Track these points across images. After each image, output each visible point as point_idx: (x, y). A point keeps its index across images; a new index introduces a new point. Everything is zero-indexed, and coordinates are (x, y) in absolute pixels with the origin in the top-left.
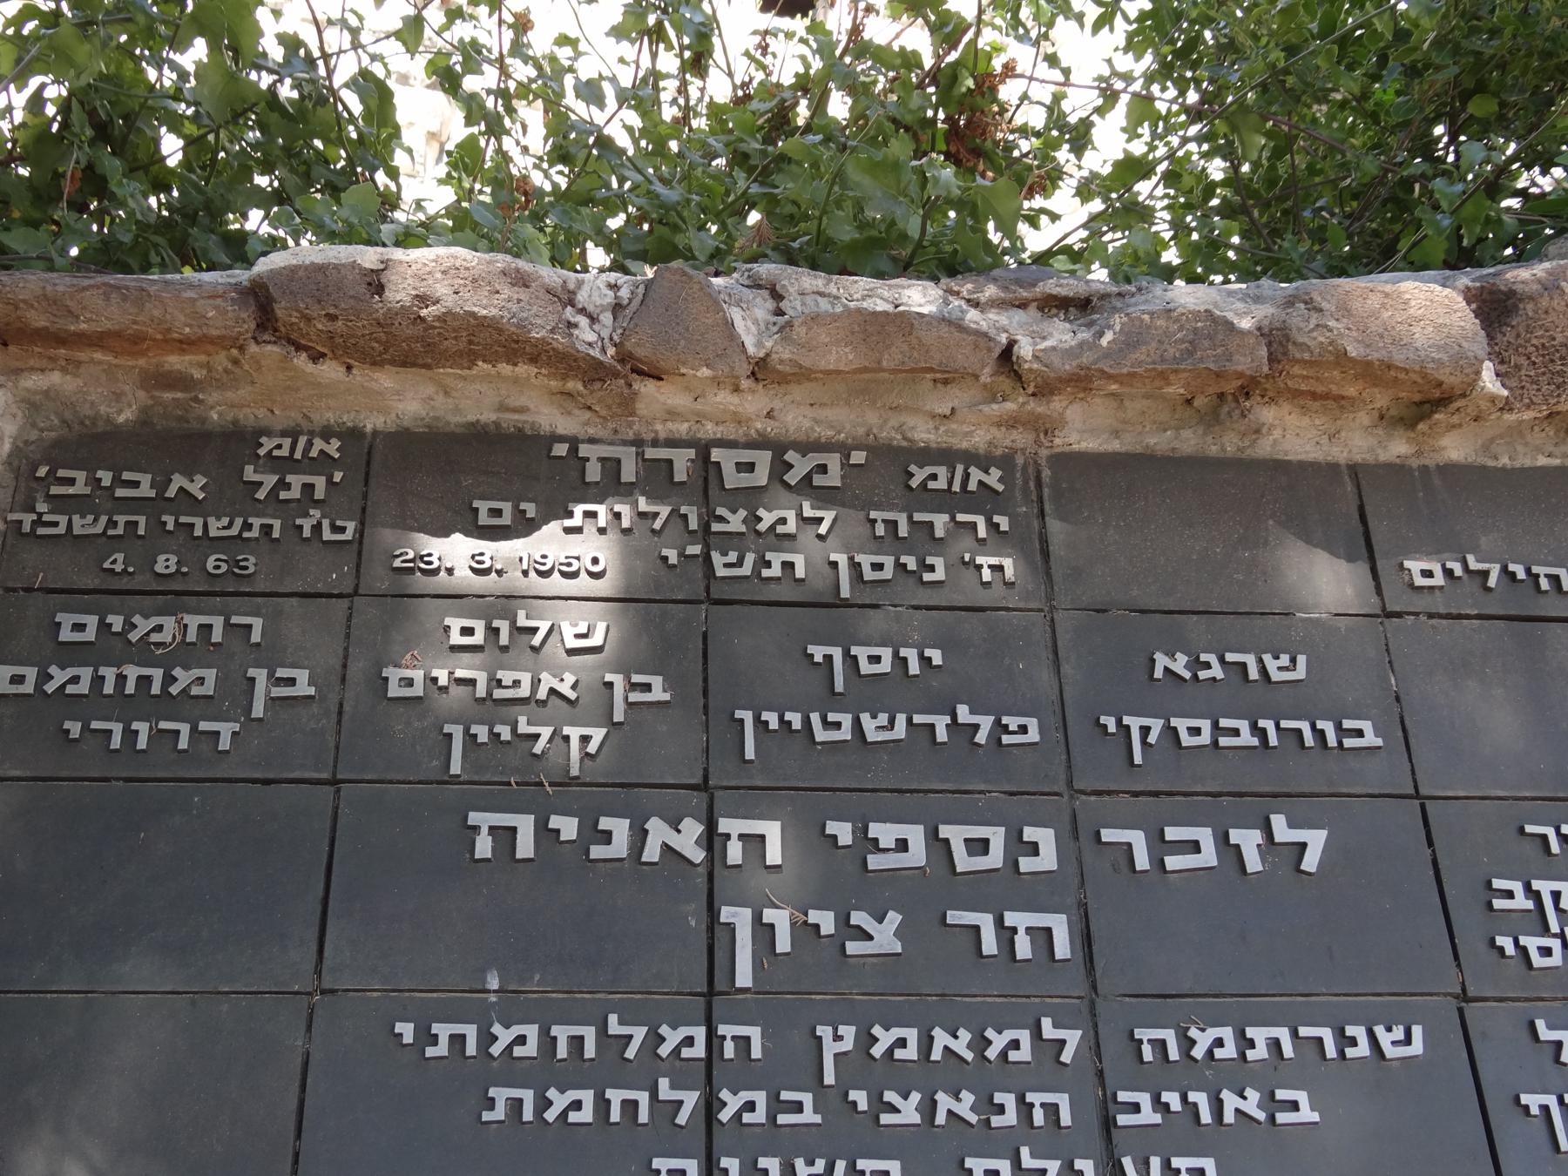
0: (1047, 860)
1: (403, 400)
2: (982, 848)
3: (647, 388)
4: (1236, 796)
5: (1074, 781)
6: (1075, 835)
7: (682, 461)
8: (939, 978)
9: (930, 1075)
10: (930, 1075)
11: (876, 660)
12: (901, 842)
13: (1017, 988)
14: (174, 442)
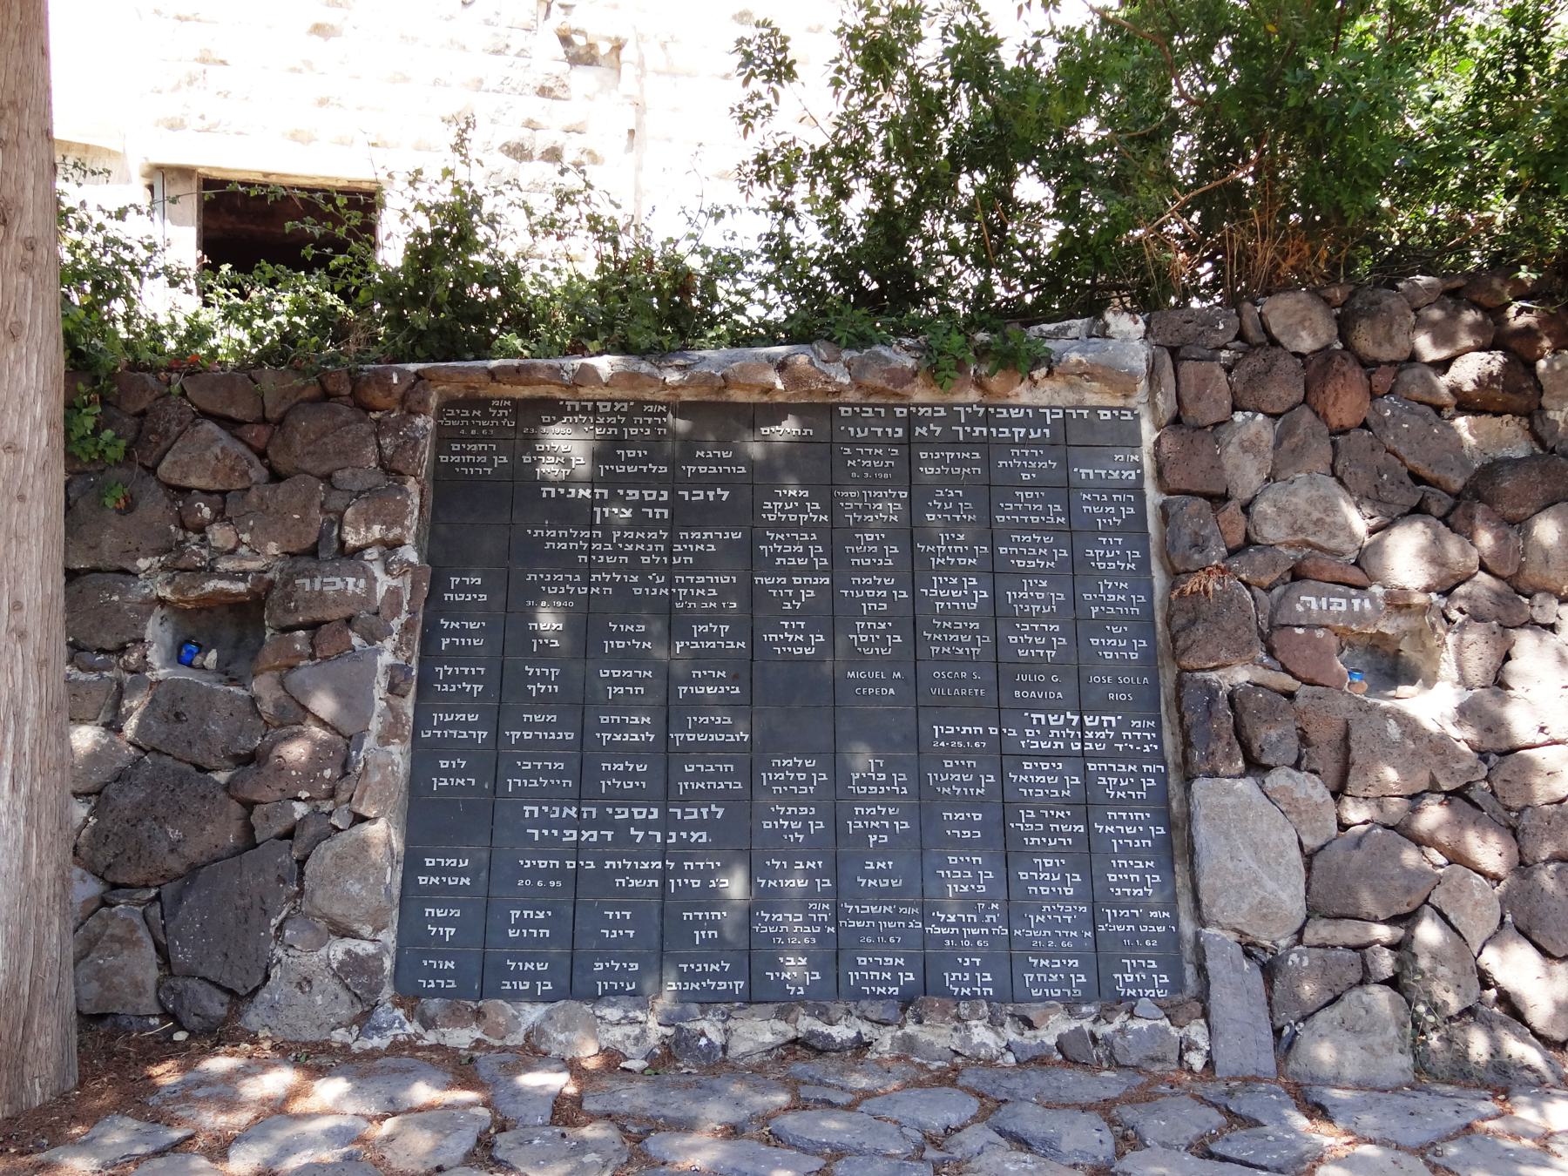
0: (665, 498)
1: (524, 392)
2: (650, 495)
3: (581, 390)
4: (708, 483)
5: (673, 482)
6: (673, 493)
7: (590, 405)
9: (634, 541)
10: (634, 541)
11: (631, 453)
12: (634, 495)
13: (656, 524)
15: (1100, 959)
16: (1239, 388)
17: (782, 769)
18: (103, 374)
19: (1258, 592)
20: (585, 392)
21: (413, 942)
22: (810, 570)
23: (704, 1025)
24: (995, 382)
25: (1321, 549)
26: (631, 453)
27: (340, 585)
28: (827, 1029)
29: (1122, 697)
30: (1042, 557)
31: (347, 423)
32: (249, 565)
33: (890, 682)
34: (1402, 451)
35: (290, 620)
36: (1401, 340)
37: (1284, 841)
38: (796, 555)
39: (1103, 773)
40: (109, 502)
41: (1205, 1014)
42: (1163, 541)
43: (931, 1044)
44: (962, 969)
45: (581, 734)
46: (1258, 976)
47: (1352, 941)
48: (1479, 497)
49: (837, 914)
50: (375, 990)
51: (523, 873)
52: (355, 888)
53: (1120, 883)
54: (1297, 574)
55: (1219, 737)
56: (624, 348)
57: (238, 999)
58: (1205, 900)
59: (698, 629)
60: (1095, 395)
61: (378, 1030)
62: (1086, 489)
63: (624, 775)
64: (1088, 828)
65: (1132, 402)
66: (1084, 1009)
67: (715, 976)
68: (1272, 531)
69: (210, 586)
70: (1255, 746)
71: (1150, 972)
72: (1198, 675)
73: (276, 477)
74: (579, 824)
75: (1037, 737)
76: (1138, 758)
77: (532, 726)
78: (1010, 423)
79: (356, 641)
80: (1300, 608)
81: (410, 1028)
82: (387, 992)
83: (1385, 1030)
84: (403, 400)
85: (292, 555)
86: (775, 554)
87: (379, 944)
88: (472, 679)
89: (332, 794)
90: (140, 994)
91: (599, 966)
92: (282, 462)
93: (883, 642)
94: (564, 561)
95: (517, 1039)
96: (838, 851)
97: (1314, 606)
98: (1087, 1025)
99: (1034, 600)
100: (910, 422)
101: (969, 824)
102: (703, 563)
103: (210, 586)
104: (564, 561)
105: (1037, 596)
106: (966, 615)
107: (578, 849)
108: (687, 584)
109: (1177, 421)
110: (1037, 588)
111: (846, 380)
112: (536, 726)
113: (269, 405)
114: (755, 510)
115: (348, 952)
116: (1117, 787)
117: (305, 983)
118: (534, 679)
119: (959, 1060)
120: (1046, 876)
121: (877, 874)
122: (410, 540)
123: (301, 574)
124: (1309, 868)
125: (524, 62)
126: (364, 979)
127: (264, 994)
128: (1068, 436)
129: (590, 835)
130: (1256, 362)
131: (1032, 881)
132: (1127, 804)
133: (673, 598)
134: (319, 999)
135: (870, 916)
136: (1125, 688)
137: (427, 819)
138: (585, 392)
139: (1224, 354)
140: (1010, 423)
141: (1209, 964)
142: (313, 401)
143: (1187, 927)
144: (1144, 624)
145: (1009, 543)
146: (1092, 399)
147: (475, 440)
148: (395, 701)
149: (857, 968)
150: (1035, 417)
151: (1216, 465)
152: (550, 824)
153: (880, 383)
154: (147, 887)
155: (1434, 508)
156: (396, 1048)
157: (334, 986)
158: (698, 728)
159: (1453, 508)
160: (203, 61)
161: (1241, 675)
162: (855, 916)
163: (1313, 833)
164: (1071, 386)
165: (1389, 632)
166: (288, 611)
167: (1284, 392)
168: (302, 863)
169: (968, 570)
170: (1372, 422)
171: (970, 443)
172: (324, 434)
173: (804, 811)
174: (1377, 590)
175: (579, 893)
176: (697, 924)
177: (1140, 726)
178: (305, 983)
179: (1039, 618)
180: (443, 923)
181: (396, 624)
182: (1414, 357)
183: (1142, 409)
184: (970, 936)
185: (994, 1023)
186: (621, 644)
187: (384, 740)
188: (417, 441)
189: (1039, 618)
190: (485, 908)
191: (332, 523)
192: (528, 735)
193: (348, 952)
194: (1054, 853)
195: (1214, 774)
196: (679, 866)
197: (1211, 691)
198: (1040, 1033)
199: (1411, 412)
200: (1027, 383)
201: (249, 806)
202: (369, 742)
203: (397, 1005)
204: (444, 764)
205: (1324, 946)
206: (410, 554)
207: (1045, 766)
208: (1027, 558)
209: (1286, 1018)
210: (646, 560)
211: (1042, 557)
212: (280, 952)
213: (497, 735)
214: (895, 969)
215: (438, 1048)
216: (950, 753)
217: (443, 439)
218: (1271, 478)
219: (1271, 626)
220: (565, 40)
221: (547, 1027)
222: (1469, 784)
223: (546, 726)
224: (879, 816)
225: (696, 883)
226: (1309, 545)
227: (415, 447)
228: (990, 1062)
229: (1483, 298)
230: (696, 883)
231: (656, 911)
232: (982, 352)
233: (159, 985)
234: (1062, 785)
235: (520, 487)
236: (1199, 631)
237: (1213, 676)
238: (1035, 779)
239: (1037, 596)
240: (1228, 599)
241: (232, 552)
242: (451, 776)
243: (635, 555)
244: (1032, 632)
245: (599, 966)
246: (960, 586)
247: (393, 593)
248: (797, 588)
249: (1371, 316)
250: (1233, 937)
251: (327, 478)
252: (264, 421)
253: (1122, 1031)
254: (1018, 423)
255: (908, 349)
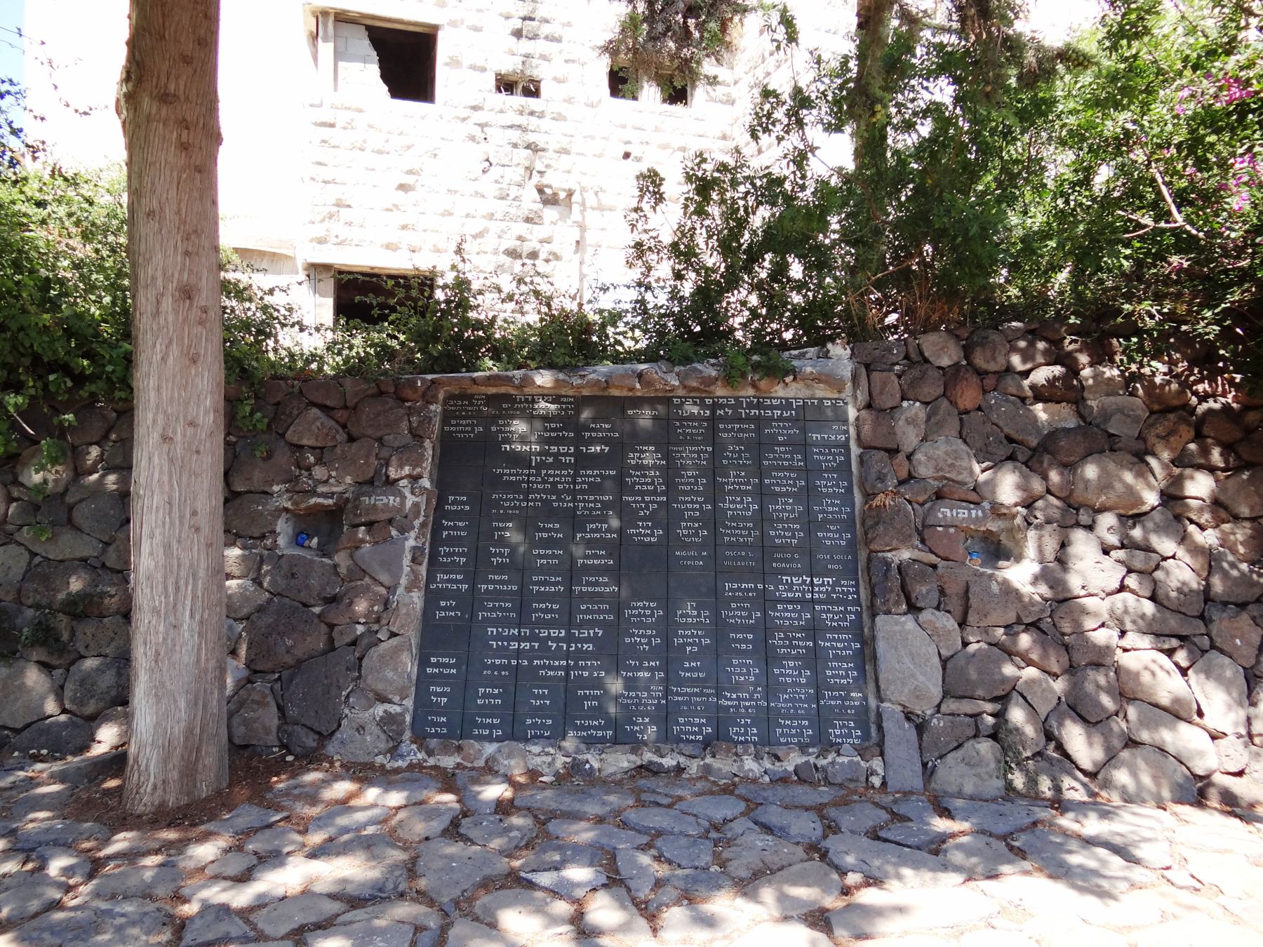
1: (493, 390)
2: (563, 449)
6: (577, 448)
8: (558, 465)
9: (554, 476)
10: (554, 476)
11: (553, 425)
12: (554, 449)
13: (566, 466)
14: (464, 396)
15: (821, 721)
16: (906, 387)
17: (637, 608)
18: (256, 382)
19: (916, 506)
20: (527, 390)
21: (423, 705)
22: (654, 493)
23: (589, 756)
24: (763, 384)
25: (953, 481)
26: (553, 425)
27: (385, 501)
28: (659, 760)
29: (836, 567)
30: (790, 485)
31: (391, 409)
32: (335, 489)
33: (700, 558)
34: (1001, 424)
35: (357, 521)
36: (1001, 360)
37: (930, 652)
38: (647, 484)
39: (824, 612)
40: (258, 454)
41: (882, 754)
42: (861, 476)
43: (720, 769)
44: (740, 726)
45: (522, 587)
46: (914, 732)
47: (970, 712)
48: (1047, 451)
49: (667, 693)
50: (401, 733)
51: (487, 667)
52: (390, 674)
53: (833, 676)
54: (939, 496)
55: (892, 591)
56: (550, 366)
57: (324, 738)
58: (882, 687)
59: (590, 526)
60: (821, 391)
61: (402, 756)
62: (816, 446)
63: (546, 611)
64: (815, 644)
65: (843, 396)
66: (811, 750)
67: (595, 728)
68: (924, 471)
69: (313, 501)
70: (913, 596)
71: (849, 728)
72: (880, 554)
73: (351, 439)
74: (519, 639)
75: (785, 590)
76: (844, 602)
77: (493, 582)
78: (772, 407)
79: (394, 533)
80: (940, 515)
81: (420, 756)
82: (407, 735)
83: (988, 765)
84: (424, 395)
85: (360, 483)
86: (635, 483)
87: (404, 707)
88: (459, 555)
89: (378, 621)
90: (267, 734)
91: (529, 721)
92: (355, 431)
93: (696, 534)
94: (514, 487)
95: (480, 763)
96: (668, 656)
97: (949, 514)
98: (812, 759)
99: (784, 510)
100: (715, 407)
101: (745, 641)
102: (595, 488)
103: (313, 501)
104: (514, 487)
105: (786, 508)
106: (745, 519)
107: (519, 654)
108: (584, 501)
109: (869, 406)
110: (786, 503)
111: (677, 383)
112: (496, 582)
113: (348, 398)
114: (624, 457)
115: (385, 711)
116: (832, 620)
117: (361, 729)
118: (495, 555)
119: (736, 779)
120: (789, 671)
121: (691, 670)
122: (426, 475)
123: (363, 494)
124: (944, 668)
125: (517, 203)
126: (394, 727)
127: (338, 735)
128: (807, 416)
129: (526, 645)
130: (915, 372)
131: (781, 674)
132: (838, 630)
133: (576, 508)
134: (368, 738)
135: (686, 694)
136: (838, 562)
137: (434, 636)
138: (527, 390)
139: (897, 367)
140: (772, 407)
141: (884, 724)
142: (373, 396)
143: (873, 703)
144: (849, 524)
145: (771, 477)
146: (820, 394)
147: (465, 418)
148: (415, 567)
149: (678, 724)
150: (787, 405)
151: (892, 432)
152: (503, 639)
153: (695, 384)
154: (273, 672)
155: (1020, 458)
156: (411, 767)
157: (377, 730)
158: (589, 584)
159: (1031, 457)
160: (338, 205)
161: (906, 555)
162: (678, 694)
163: (947, 648)
164: (808, 386)
165: (994, 530)
166: (356, 515)
167: (932, 389)
168: (361, 659)
169: (747, 493)
170: (983, 407)
171: (749, 419)
172: (378, 415)
173: (649, 632)
174: (986, 505)
175: (518, 679)
176: (586, 698)
177: (846, 585)
178: (361, 729)
179: (788, 521)
180: (440, 694)
181: (417, 523)
182: (1009, 369)
183: (849, 400)
184: (745, 707)
185: (758, 757)
186: (545, 535)
187: (409, 589)
188: (431, 419)
189: (788, 521)
190: (464, 687)
191: (382, 465)
192: (491, 587)
193: (385, 711)
194: (795, 658)
195: (888, 612)
196: (576, 664)
197: (887, 564)
198: (785, 764)
199: (1007, 401)
200: (782, 385)
201: (331, 626)
202: (400, 591)
203: (412, 742)
204: (443, 604)
205: (952, 714)
206: (426, 483)
207: (790, 607)
208: (780, 485)
209: (930, 757)
210: (560, 487)
211: (790, 485)
212: (347, 711)
213: (473, 588)
214: (700, 725)
215: (435, 767)
216: (734, 599)
217: (447, 417)
218: (924, 439)
219: (923, 526)
220: (540, 191)
221: (498, 756)
222: (1040, 619)
223: (501, 582)
224: (693, 636)
225: (586, 674)
226: (946, 478)
227: (429, 423)
228: (755, 781)
229: (1050, 335)
230: (586, 674)
231: (562, 690)
232: (756, 367)
233: (279, 728)
234: (800, 618)
235: (490, 447)
236: (881, 528)
237: (889, 555)
238: (784, 615)
239: (786, 508)
240: (898, 510)
241: (326, 482)
242: (447, 611)
243: (554, 484)
244: (783, 529)
245: (529, 721)
246: (742, 502)
247: (416, 505)
248: (647, 503)
249: (982, 345)
250: (900, 708)
251: (380, 440)
252: (346, 407)
253: (833, 763)
254: (776, 407)
255: (713, 365)
